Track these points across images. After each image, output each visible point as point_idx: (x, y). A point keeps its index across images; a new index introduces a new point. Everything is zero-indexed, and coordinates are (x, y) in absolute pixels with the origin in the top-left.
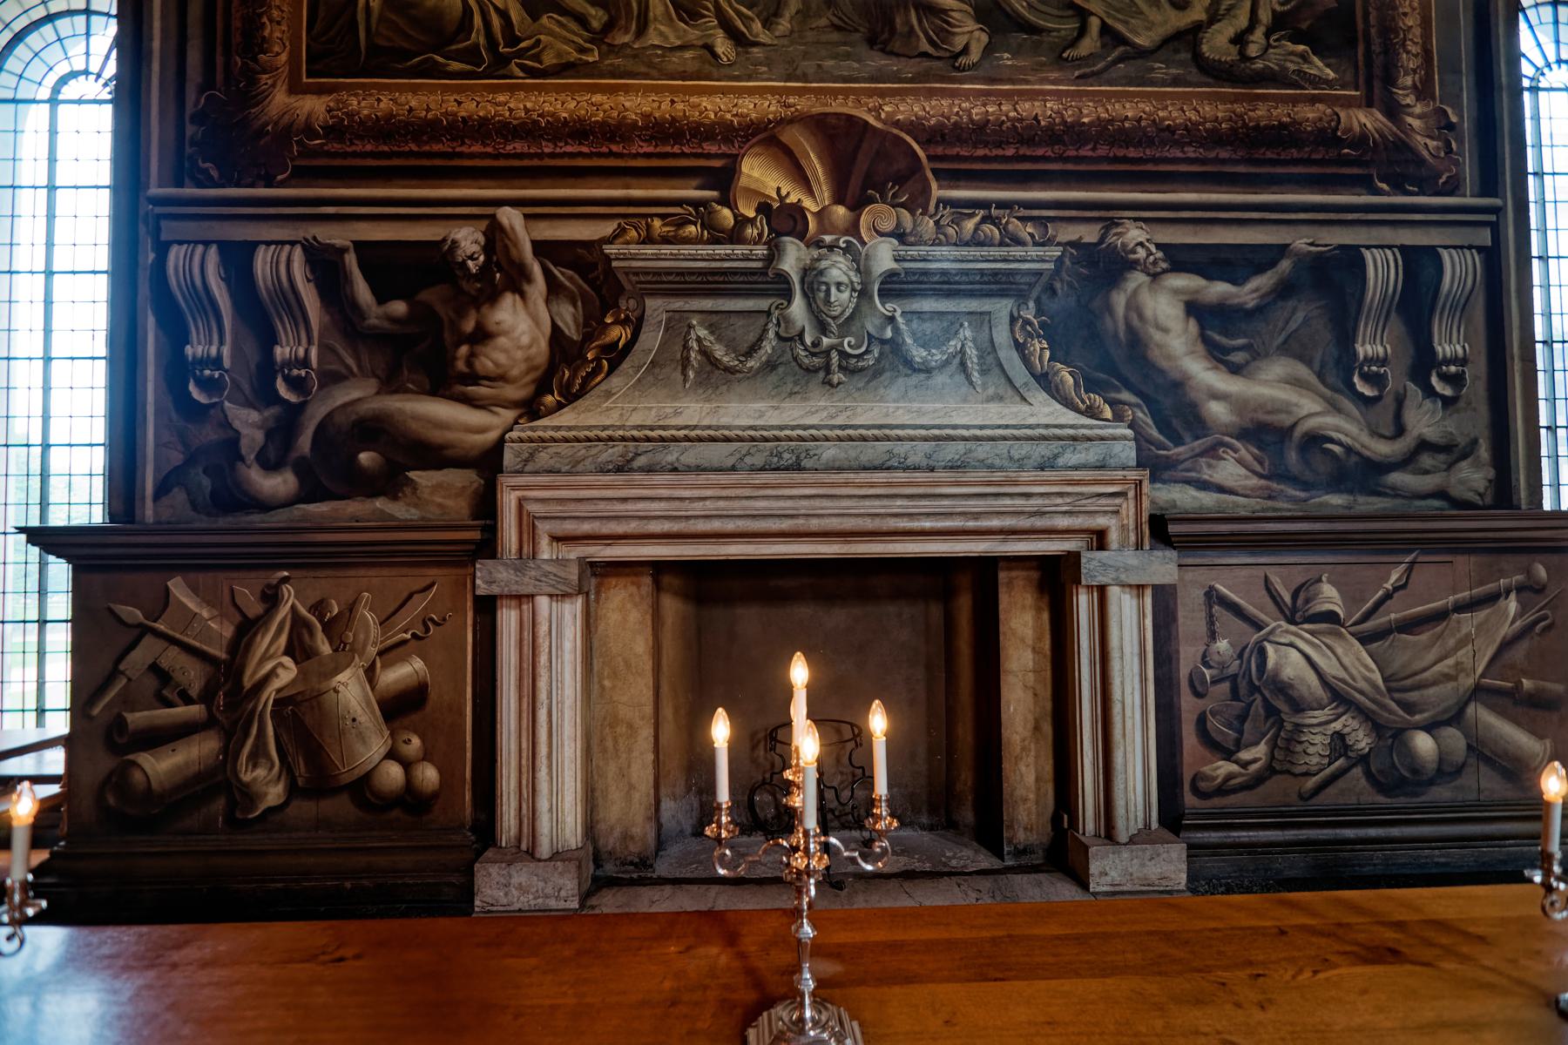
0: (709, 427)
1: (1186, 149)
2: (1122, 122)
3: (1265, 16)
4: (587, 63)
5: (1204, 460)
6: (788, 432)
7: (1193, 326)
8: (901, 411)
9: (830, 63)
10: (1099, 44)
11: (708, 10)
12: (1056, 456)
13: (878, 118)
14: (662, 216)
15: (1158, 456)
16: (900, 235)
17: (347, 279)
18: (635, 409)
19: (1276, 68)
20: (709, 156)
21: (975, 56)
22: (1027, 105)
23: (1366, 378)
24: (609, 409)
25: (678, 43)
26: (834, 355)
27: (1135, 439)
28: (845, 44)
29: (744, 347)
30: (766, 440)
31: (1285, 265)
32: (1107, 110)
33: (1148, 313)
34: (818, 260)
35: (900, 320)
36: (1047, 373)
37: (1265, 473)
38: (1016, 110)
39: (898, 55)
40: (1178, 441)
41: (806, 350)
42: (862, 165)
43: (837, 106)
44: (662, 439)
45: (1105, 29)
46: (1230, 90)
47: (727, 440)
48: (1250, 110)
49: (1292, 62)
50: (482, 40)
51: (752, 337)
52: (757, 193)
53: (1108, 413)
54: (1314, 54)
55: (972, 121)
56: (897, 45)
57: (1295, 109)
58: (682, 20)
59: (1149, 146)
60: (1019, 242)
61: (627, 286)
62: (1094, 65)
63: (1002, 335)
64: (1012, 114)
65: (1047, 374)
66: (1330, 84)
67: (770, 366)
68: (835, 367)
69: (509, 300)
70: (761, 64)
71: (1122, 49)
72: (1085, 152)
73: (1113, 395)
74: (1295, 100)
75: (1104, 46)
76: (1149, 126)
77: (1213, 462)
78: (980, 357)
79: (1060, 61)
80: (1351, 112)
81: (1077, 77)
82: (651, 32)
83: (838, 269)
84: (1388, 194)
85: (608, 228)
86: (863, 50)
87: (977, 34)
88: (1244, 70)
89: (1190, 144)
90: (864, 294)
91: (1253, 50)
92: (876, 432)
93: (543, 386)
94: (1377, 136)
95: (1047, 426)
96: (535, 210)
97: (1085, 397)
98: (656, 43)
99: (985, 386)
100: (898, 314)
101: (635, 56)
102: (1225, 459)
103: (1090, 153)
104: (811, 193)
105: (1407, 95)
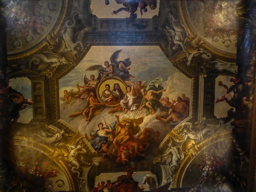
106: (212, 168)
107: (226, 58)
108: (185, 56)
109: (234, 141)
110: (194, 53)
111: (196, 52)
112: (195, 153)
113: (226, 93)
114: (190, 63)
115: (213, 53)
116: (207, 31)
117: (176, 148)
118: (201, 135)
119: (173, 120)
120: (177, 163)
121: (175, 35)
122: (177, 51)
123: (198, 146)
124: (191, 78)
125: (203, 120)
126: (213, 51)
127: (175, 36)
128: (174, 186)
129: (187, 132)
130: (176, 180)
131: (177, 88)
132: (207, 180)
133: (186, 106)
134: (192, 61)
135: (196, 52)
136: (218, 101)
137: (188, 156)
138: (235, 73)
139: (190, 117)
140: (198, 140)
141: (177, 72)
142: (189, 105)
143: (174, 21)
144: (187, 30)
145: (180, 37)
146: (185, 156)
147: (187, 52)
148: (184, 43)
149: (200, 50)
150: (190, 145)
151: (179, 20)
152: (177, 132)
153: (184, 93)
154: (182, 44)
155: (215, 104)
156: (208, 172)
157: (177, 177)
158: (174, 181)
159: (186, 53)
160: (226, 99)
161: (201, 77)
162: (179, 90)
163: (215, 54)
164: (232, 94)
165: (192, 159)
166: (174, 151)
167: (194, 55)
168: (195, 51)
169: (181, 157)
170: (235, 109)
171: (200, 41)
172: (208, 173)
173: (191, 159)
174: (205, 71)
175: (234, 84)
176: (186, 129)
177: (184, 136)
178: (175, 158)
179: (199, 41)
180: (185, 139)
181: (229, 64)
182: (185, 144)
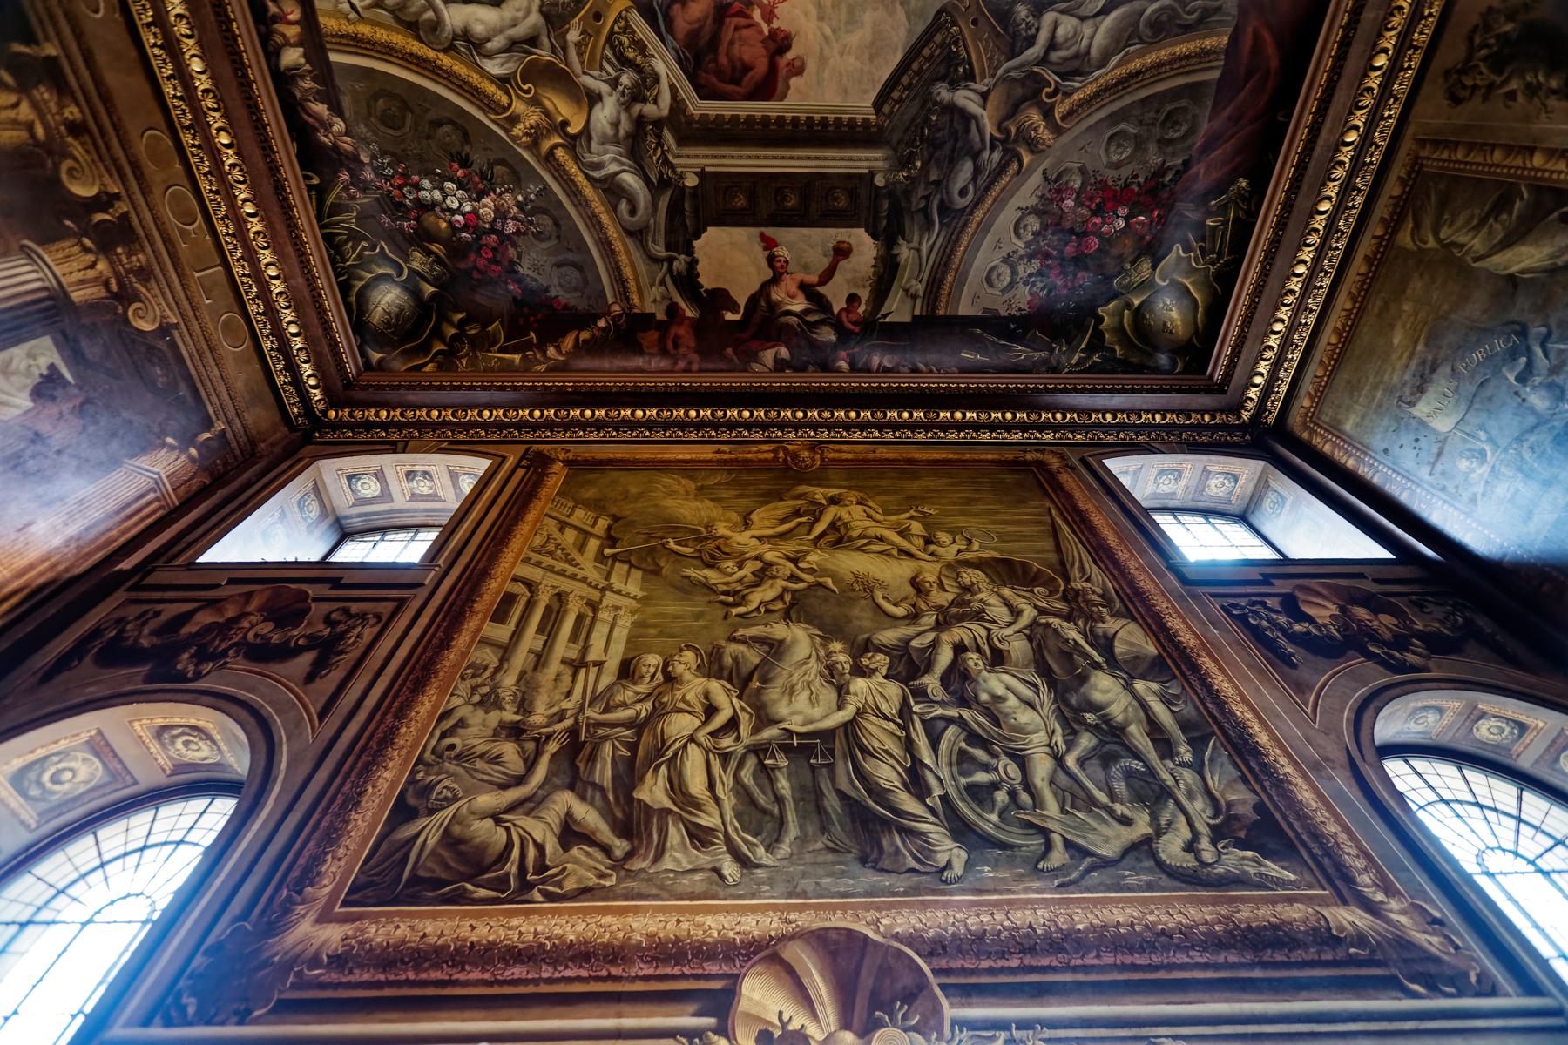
3: (1202, 828)
4: (604, 887)
9: (828, 880)
11: (718, 838)
13: (877, 931)
21: (958, 869)
22: (1019, 914)
25: (690, 867)
28: (840, 863)
39: (888, 872)
42: (866, 981)
43: (837, 921)
45: (1068, 844)
50: (514, 870)
56: (886, 863)
58: (695, 848)
62: (1069, 874)
64: (1007, 923)
70: (764, 884)
71: (1089, 859)
72: (1090, 960)
74: (1273, 901)
75: (1072, 857)
79: (1036, 872)
81: (1058, 886)
82: (667, 856)
86: (856, 867)
87: (956, 851)
88: (1208, 875)
89: (1192, 947)
98: (670, 867)
101: (649, 880)
103: (1096, 962)
106: (465, 228)
107: (945, 273)
108: (977, 71)
109: (602, 323)
110: (986, 121)
111: (989, 128)
112: (524, 139)
113: (800, 276)
114: (942, 101)
115: (972, 213)
116: (1067, 182)
117: (535, 27)
118: (613, 168)
119: (677, 7)
120: (455, 37)
121: (1083, 19)
122: (1005, 29)
123: (560, 153)
124: (878, 105)
125: (682, 176)
126: (979, 215)
127: (1072, 15)
128: (330, 14)
129: (621, 88)
130: (365, 30)
131: (834, 31)
132: (402, 204)
133: (746, 79)
134: (952, 109)
135: (989, 128)
136: (769, 243)
137: (504, 100)
138: (883, 311)
139: (698, 107)
140: (590, 152)
141: (909, 31)
142: (751, 96)
143: (1145, 10)
144: (1090, 83)
145: (1068, 44)
146: (503, 81)
147: (994, 85)
148: (1036, 69)
149: (993, 148)
150: (562, 107)
151: (1142, 42)
152: (616, 29)
153: (811, 66)
154: (1031, 59)
155: (755, 231)
156: (443, 211)
157: (381, 35)
158: (353, 15)
159: (993, 76)
160: (776, 280)
161: (877, 159)
162: (826, 39)
163: (965, 225)
164: (799, 305)
165: (493, 121)
166: (520, 14)
167: (975, 118)
168: (992, 124)
169: (489, 56)
170: (737, 317)
171: (1032, 152)
172: (437, 209)
173: (493, 116)
174: (902, 175)
175: (836, 311)
176: (635, 85)
177: (604, 73)
178: (482, 22)
179: (1033, 145)
180: (587, 81)
181: (920, 288)
182: (560, 79)
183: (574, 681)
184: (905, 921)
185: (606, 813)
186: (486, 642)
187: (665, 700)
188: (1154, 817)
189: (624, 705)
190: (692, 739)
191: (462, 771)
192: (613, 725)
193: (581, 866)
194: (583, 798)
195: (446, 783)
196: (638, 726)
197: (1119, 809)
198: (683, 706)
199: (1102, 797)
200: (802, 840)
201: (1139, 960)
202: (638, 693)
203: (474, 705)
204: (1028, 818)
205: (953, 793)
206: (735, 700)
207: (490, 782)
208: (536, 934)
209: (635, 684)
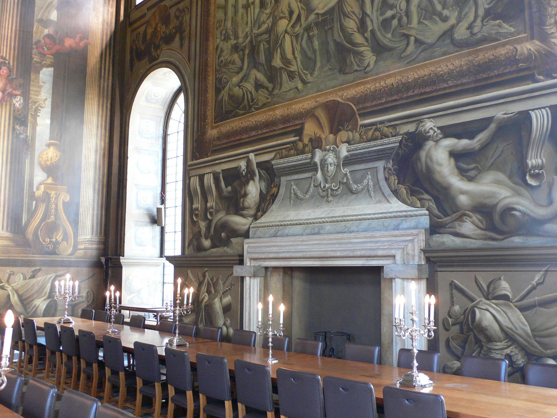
0: (296, 220)
1: (448, 83)
2: (423, 77)
3: (481, 12)
4: (269, 102)
5: (457, 222)
6: (316, 220)
7: (452, 161)
8: (348, 210)
10: (414, 47)
12: (399, 225)
13: (342, 99)
14: (285, 148)
15: (438, 222)
16: (348, 142)
17: (220, 182)
18: (278, 215)
19: (487, 35)
20: (296, 125)
21: (372, 66)
23: (533, 176)
24: (272, 216)
26: (329, 190)
27: (429, 215)
29: (305, 191)
30: (311, 224)
31: (493, 126)
32: (418, 74)
33: (434, 158)
34: (325, 156)
35: (348, 174)
36: (396, 190)
37: (483, 227)
38: (385, 83)
40: (447, 215)
41: (322, 189)
44: (285, 225)
45: (417, 40)
46: (467, 51)
47: (301, 224)
48: (476, 57)
49: (494, 29)
50: (247, 102)
51: (307, 187)
52: (308, 134)
53: (419, 204)
54: (504, 23)
55: (371, 92)
57: (496, 51)
58: (290, 81)
59: (433, 85)
60: (387, 136)
61: (277, 174)
63: (381, 175)
64: (385, 85)
65: (396, 190)
66: (512, 34)
67: (312, 197)
68: (329, 195)
69: (251, 182)
71: (423, 47)
72: (410, 94)
73: (421, 196)
74: (495, 47)
75: (416, 48)
76: (434, 76)
77: (460, 223)
78: (374, 186)
79: (401, 58)
80: (523, 45)
81: (407, 63)
82: (283, 87)
83: (331, 158)
84: (543, 81)
85: (272, 155)
89: (450, 80)
90: (338, 166)
91: (476, 30)
92: (341, 218)
93: (258, 210)
94: (536, 53)
95: (397, 212)
96: (258, 152)
97: (410, 198)
99: (375, 198)
100: (348, 172)
102: (466, 222)
103: (412, 94)
104: (323, 131)
105: (552, 28)
183: (247, 17)
184: (352, 92)
185: (265, 75)
186: (219, 7)
187: (276, 14)
188: (460, 13)
189: (264, 22)
190: (286, 32)
191: (226, 70)
192: (261, 34)
193: (262, 96)
194: (258, 71)
195: (224, 76)
196: (269, 31)
197: (446, 12)
198: (282, 15)
199: (439, 7)
200: (321, 68)
201: (428, 89)
202: (267, 14)
203: (223, 41)
204: (404, 31)
205: (376, 28)
206: (299, 3)
207: (235, 72)
208: (256, 121)
209: (266, 9)
